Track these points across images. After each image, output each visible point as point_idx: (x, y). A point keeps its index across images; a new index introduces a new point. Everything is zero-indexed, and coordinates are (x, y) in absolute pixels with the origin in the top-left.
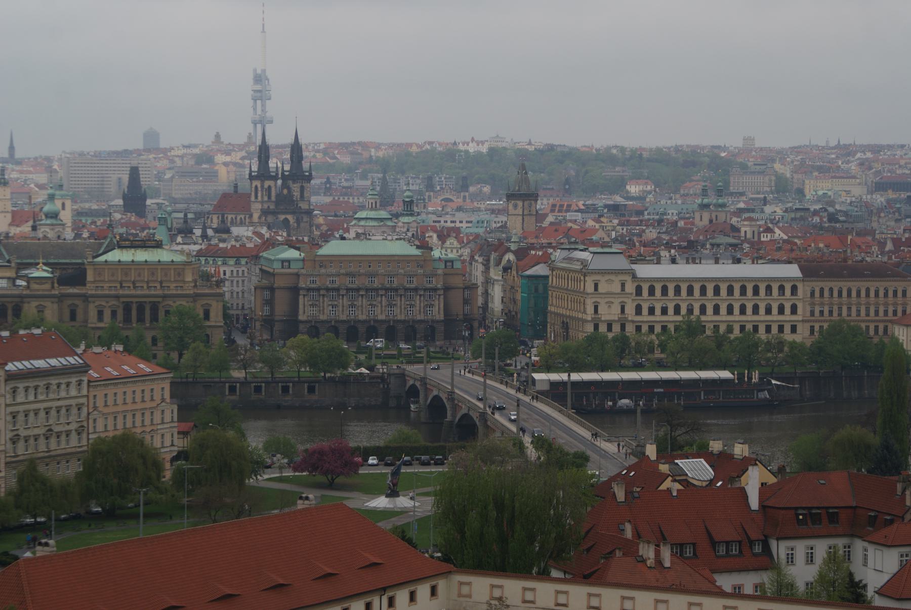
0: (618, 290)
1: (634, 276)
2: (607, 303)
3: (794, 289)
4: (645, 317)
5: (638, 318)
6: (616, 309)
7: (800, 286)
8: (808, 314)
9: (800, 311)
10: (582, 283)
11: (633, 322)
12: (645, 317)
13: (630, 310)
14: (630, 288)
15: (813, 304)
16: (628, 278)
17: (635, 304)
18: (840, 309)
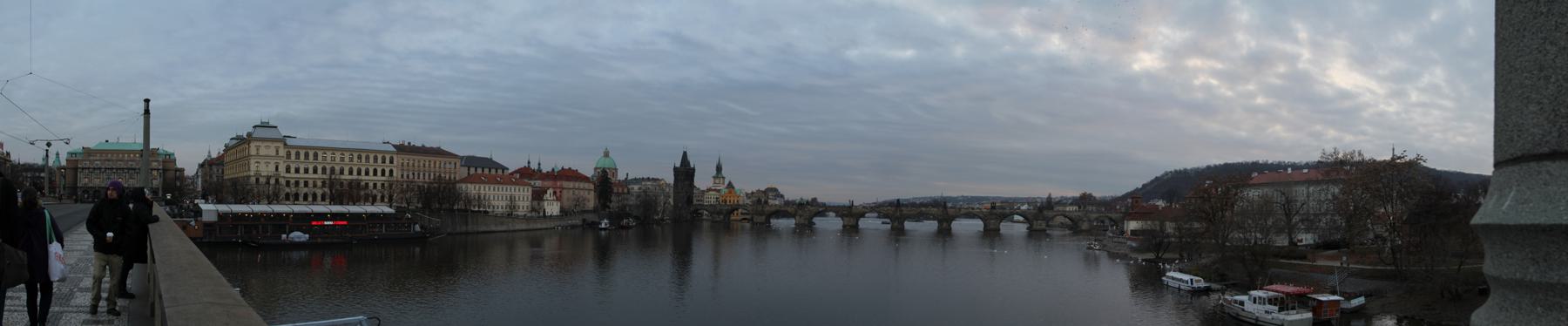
0: (274, 154)
1: (285, 144)
2: (266, 163)
3: (391, 162)
4: (293, 174)
5: (288, 175)
6: (272, 168)
7: (395, 157)
8: (400, 176)
9: (395, 174)
10: (247, 151)
11: (284, 177)
12: (293, 174)
13: (282, 169)
14: (282, 152)
15: (403, 170)
16: (281, 145)
17: (286, 164)
18: (424, 175)
